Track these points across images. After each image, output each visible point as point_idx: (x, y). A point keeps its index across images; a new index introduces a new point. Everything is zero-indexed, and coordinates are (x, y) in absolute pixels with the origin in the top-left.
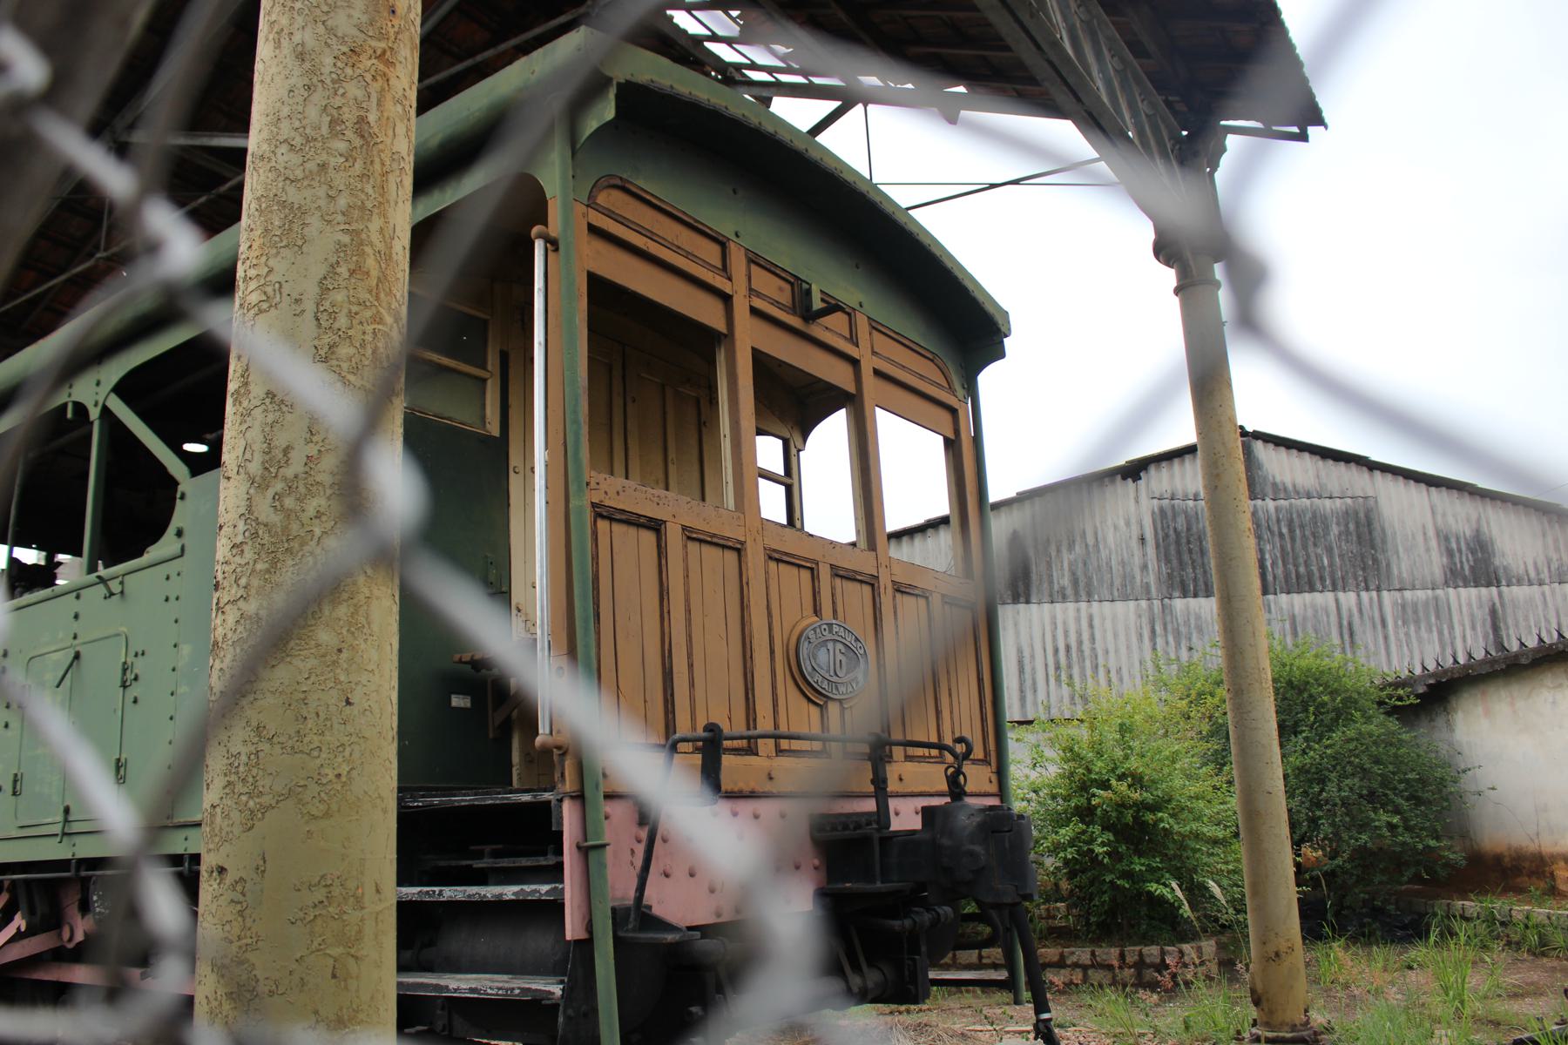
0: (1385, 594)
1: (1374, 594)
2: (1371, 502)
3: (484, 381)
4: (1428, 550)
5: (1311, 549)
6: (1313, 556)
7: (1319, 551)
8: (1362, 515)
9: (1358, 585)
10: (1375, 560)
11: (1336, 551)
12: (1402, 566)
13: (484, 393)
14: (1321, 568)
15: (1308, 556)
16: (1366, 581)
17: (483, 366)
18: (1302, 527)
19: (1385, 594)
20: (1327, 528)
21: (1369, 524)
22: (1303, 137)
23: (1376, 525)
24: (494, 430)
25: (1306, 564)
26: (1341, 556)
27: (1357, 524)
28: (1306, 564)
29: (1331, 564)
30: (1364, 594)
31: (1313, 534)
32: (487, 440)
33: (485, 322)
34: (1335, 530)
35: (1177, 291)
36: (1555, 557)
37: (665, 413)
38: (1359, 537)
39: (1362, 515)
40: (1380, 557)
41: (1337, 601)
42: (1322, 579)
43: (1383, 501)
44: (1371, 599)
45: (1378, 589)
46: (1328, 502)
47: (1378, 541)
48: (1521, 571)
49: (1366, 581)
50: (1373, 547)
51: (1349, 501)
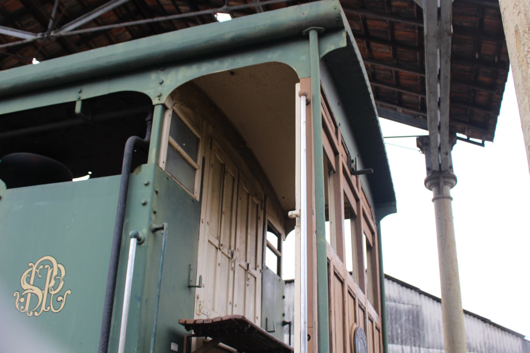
0: (422, 349)
1: (417, 348)
2: (419, 308)
3: (195, 170)
4: (440, 332)
5: (394, 325)
6: (394, 328)
7: (397, 326)
8: (415, 313)
9: (411, 344)
10: (419, 333)
11: (404, 328)
12: (429, 338)
13: (194, 177)
14: (397, 334)
15: (392, 328)
16: (414, 342)
17: (196, 161)
18: (391, 314)
19: (422, 349)
20: (401, 317)
21: (418, 317)
22: (482, 145)
23: (420, 318)
24: (197, 196)
25: (392, 332)
26: (406, 330)
27: (413, 316)
28: (392, 332)
29: (401, 333)
30: (413, 348)
31: (395, 318)
32: (194, 200)
33: (198, 139)
34: (404, 318)
35: (433, 200)
36: (487, 341)
37: (248, 209)
38: (413, 322)
39: (415, 313)
40: (421, 332)
41: (402, 349)
42: (397, 339)
43: (424, 308)
44: (416, 351)
45: (419, 346)
46: (402, 306)
47: (421, 325)
48: (475, 346)
49: (414, 342)
50: (418, 327)
51: (410, 306)
